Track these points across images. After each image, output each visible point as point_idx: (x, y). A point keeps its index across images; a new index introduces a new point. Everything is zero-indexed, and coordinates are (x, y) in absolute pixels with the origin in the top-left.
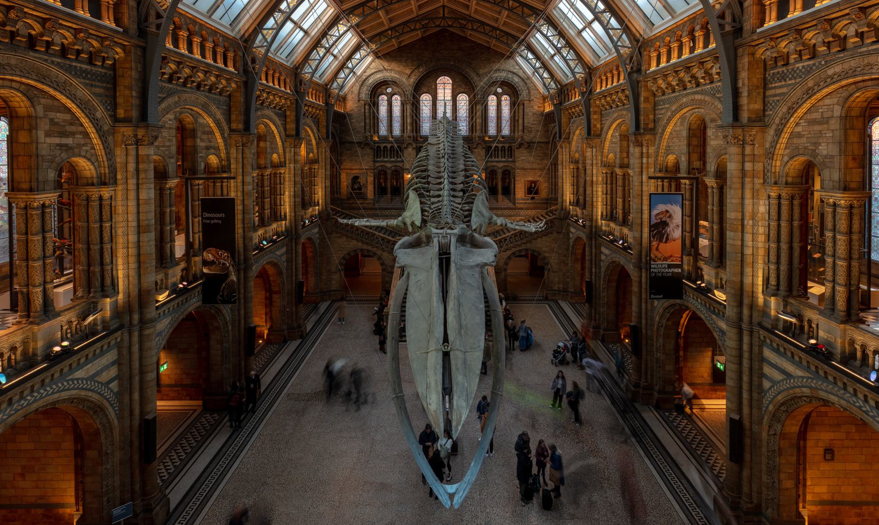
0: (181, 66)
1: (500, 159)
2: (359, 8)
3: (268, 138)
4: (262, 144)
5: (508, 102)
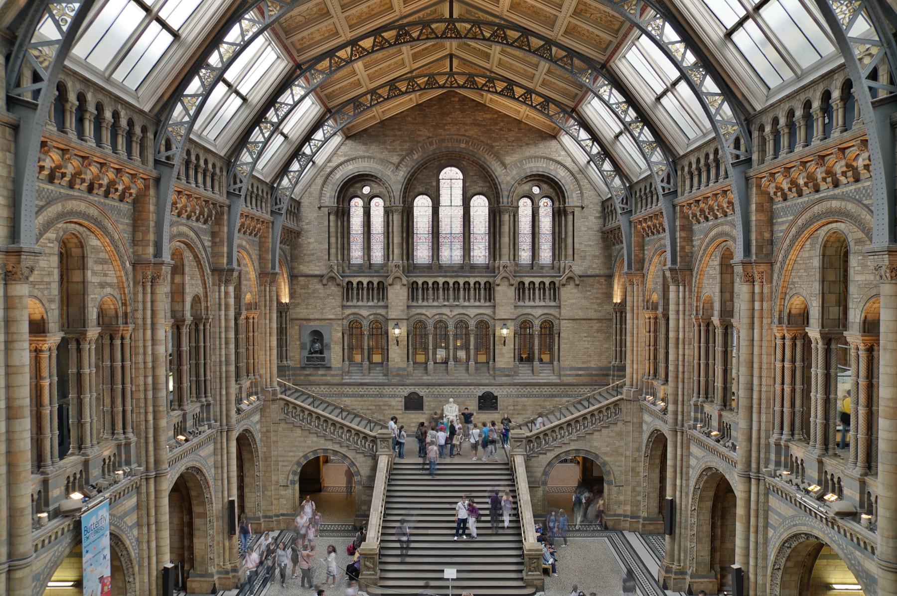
0: (67, 156)
1: (537, 303)
2: (324, 59)
3: (187, 269)
4: (178, 279)
5: (550, 210)
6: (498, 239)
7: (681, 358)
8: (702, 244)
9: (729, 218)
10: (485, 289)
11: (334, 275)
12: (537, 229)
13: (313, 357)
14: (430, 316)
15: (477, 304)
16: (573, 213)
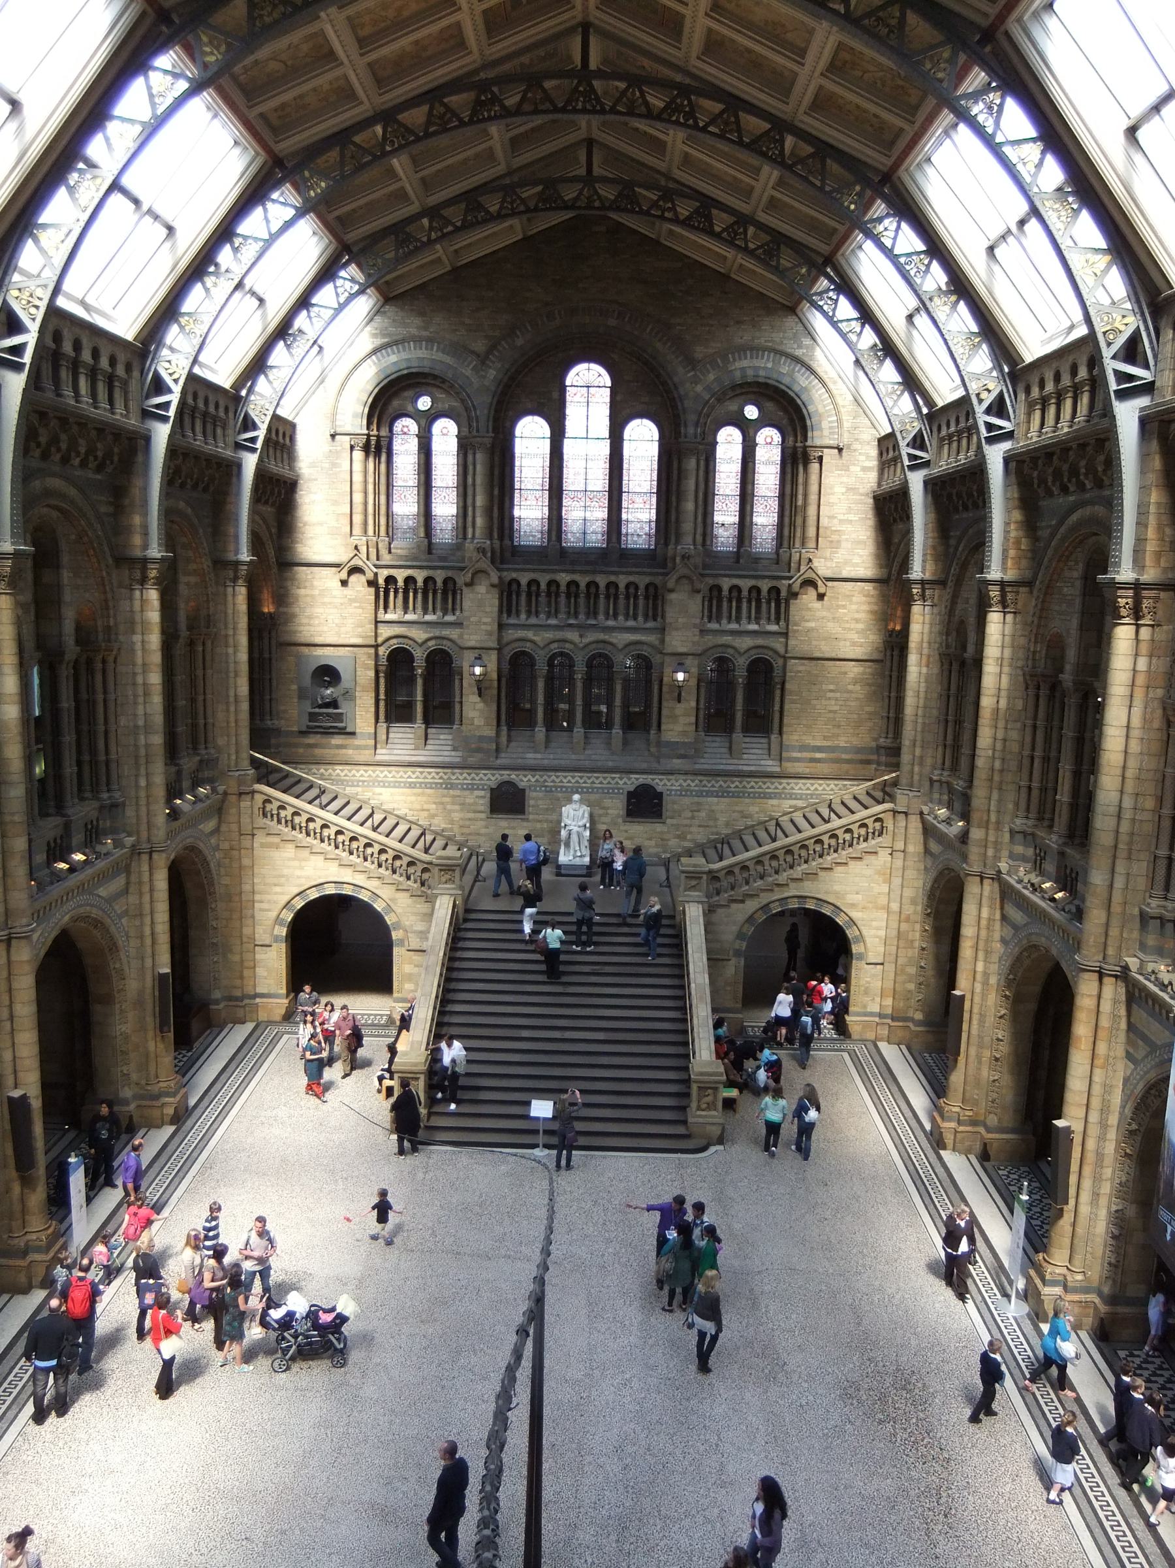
6: (674, 504)
7: (999, 746)
8: (1053, 535)
9: (1107, 493)
10: (647, 598)
11: (360, 563)
12: (750, 487)
13: (321, 714)
14: (542, 645)
15: (631, 623)
16: (821, 459)
